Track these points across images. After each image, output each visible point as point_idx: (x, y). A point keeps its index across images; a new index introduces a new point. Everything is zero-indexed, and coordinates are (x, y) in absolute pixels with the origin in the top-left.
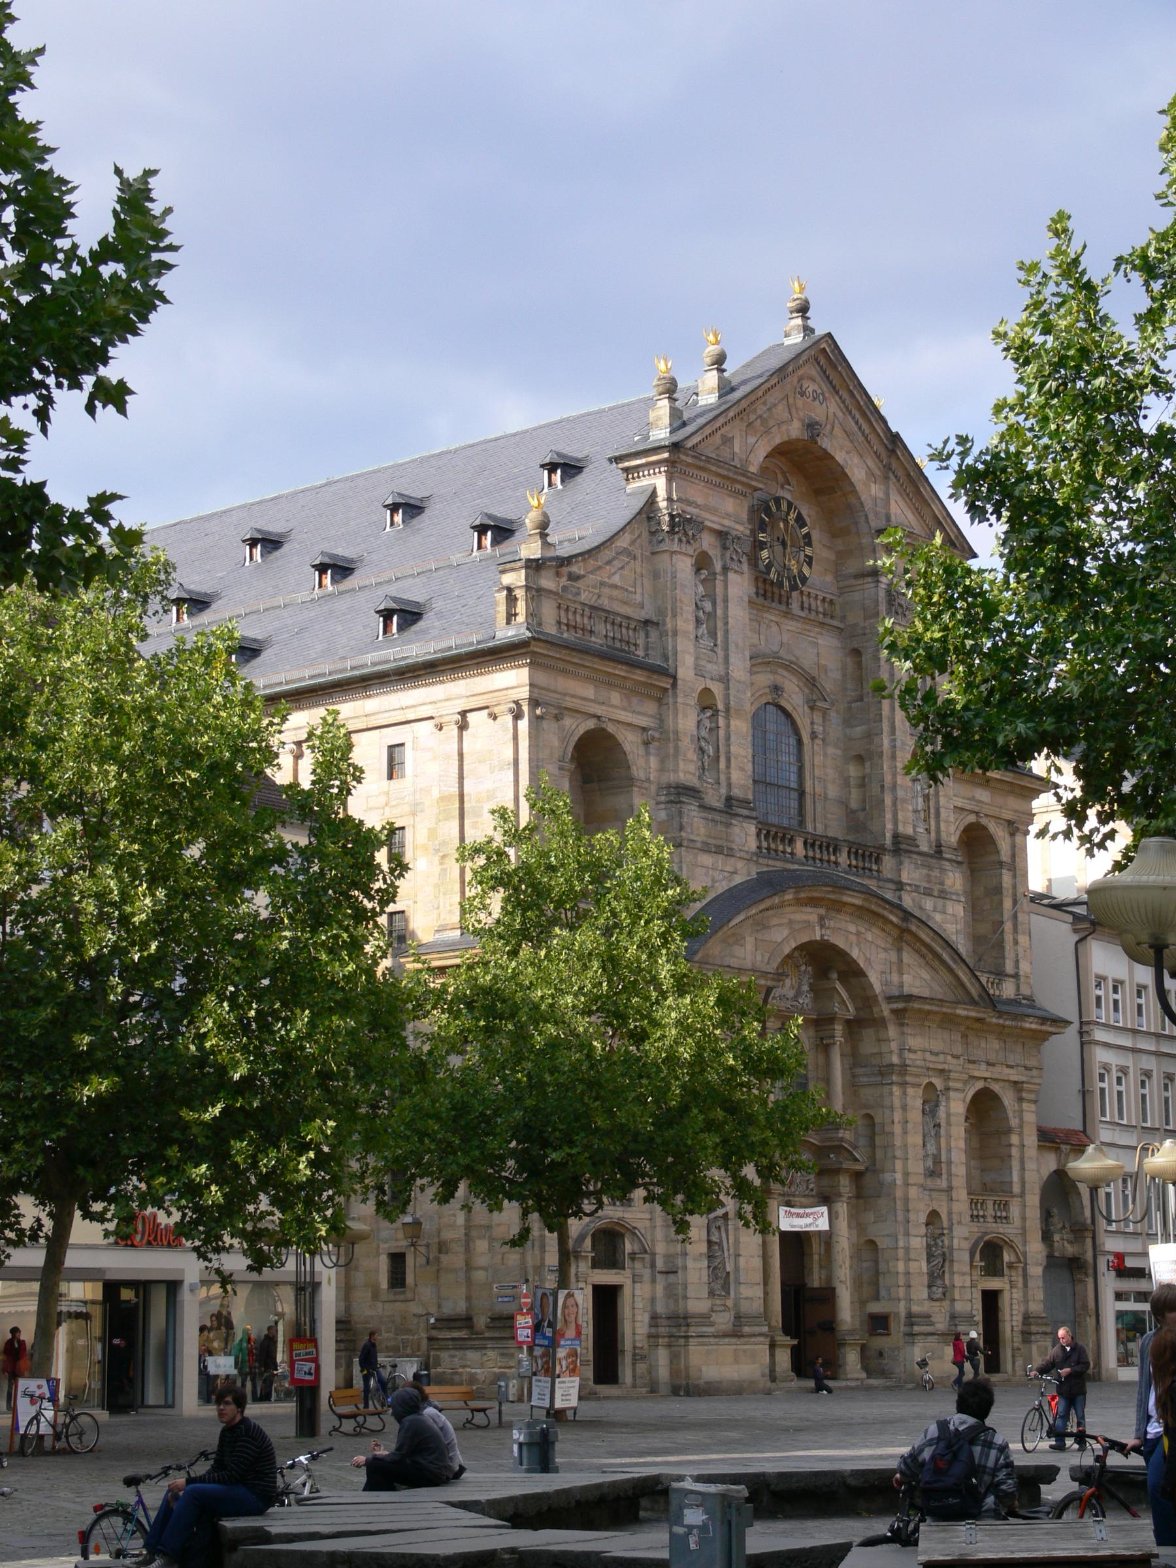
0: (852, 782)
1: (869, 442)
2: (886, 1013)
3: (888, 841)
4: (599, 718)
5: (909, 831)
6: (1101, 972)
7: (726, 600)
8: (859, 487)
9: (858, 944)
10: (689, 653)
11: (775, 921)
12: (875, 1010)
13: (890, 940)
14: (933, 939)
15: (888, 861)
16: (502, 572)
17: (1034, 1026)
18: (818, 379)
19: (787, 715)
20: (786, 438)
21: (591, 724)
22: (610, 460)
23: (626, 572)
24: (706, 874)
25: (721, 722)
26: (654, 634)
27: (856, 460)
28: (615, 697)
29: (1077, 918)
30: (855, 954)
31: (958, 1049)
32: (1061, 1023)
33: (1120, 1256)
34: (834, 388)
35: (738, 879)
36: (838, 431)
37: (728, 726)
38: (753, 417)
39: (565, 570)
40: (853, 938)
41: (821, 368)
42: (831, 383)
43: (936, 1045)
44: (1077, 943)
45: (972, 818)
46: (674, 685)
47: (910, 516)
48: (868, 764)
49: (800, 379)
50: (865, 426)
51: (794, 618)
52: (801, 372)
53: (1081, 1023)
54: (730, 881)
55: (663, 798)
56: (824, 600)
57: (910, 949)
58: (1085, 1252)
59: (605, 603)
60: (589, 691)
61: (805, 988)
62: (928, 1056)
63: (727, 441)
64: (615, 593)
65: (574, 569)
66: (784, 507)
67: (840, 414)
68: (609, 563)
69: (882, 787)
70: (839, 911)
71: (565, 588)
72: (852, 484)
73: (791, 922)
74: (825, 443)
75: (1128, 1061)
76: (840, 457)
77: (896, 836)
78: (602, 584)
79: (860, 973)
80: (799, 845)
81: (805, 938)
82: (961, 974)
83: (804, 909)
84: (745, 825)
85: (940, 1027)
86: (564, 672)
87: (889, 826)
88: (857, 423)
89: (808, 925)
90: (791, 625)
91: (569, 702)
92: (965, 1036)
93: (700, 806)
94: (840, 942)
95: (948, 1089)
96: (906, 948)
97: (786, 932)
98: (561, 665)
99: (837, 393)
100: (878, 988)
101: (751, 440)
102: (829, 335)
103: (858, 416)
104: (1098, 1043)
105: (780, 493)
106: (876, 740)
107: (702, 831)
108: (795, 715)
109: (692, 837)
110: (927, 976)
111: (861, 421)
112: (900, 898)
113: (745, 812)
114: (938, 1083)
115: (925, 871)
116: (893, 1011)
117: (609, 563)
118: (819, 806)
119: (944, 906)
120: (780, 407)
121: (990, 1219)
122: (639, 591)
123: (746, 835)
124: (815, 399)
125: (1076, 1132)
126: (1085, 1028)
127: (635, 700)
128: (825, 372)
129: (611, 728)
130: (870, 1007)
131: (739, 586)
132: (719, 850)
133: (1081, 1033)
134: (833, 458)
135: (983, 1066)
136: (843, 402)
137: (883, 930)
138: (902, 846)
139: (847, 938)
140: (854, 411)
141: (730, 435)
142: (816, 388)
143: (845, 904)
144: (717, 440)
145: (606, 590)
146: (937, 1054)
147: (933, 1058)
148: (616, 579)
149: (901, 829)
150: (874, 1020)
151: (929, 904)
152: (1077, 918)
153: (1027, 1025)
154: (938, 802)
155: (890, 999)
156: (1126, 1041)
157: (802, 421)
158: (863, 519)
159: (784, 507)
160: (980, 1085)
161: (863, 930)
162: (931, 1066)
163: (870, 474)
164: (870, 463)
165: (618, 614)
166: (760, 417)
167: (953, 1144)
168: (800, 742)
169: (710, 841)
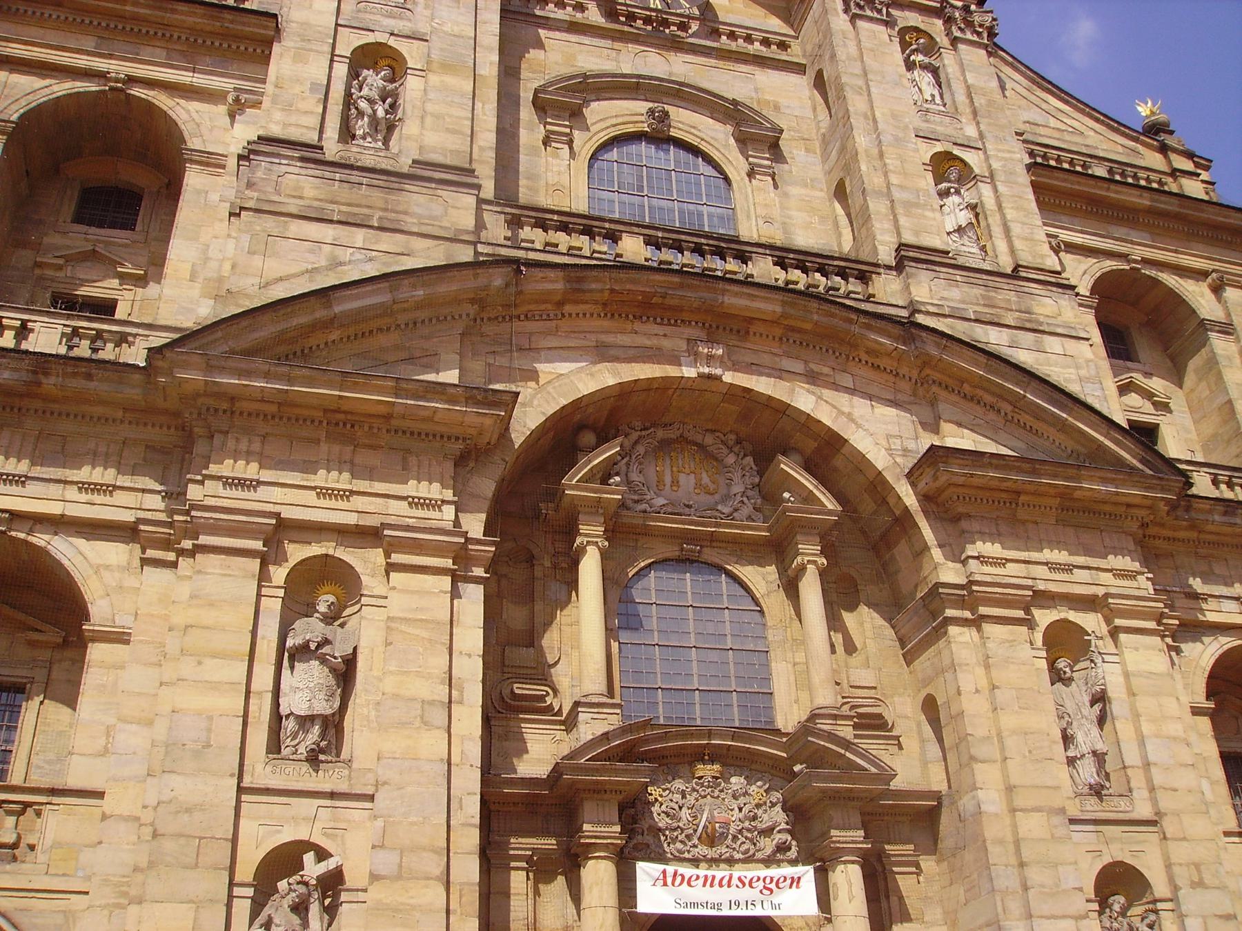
12: (891, 501)
13: (905, 386)
14: (988, 369)
24: (311, 251)
57: (954, 398)
69: (864, 191)
79: (833, 442)
83: (638, 326)
84: (439, 192)
93: (302, 159)
95: (1114, 633)
96: (943, 394)
100: (879, 459)
108: (704, 147)
109: (276, 198)
114: (1091, 622)
115: (977, 291)
130: (884, 502)
149: (909, 238)
154: (1003, 216)
161: (826, 370)
167: (1146, 728)
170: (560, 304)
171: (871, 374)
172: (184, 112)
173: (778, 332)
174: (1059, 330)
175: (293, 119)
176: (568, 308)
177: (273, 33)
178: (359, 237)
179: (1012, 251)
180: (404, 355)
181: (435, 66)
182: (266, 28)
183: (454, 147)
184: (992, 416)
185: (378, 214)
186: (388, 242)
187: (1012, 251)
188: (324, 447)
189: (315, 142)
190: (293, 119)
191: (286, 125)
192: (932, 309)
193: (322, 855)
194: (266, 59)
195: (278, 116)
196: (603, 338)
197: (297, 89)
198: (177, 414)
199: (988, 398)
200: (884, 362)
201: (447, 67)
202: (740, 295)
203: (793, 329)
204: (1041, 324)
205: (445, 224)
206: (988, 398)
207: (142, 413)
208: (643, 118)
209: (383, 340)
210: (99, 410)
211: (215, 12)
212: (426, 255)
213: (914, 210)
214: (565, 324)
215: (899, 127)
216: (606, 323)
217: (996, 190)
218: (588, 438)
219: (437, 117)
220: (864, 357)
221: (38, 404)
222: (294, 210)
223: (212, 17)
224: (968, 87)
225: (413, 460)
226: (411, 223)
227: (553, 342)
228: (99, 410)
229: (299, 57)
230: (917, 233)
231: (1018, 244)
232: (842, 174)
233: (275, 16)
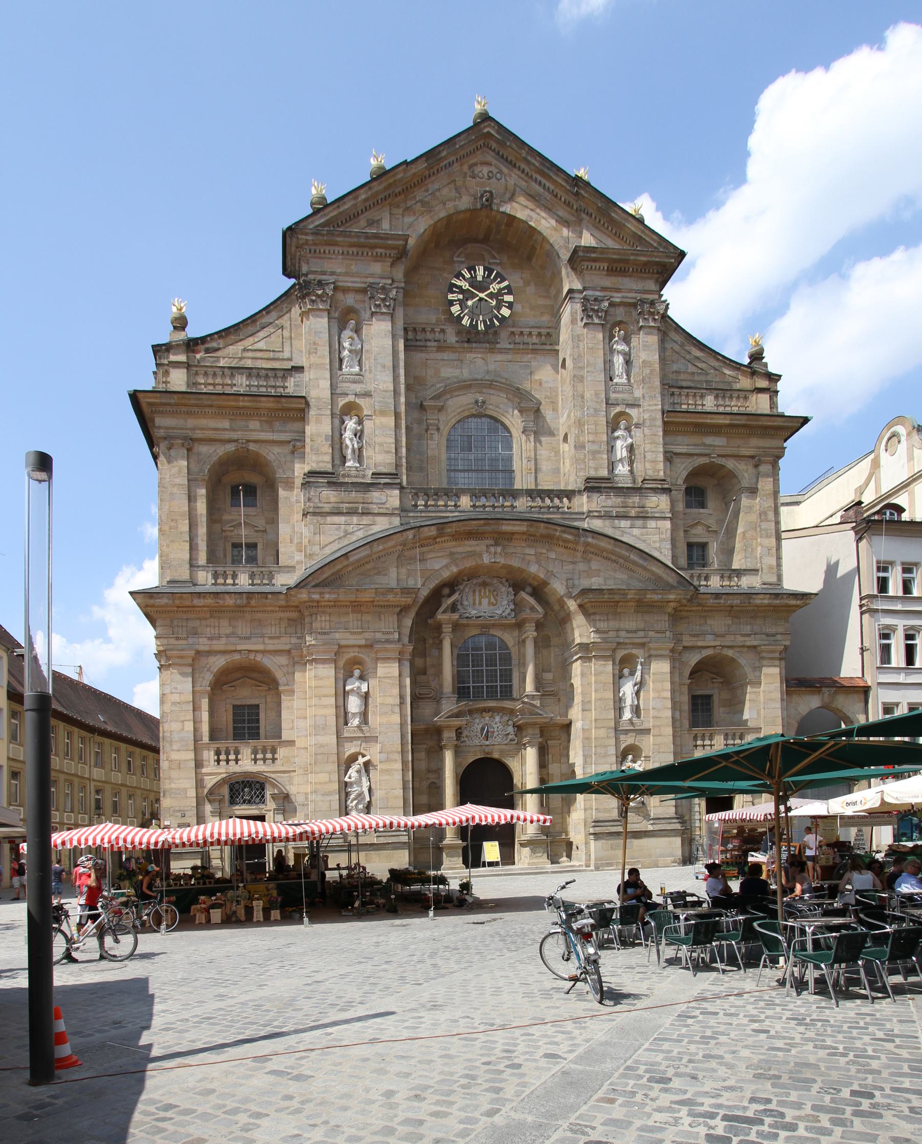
1: (556, 196)
4: (236, 441)
9: (538, 562)
10: (325, 379)
28: (254, 424)
34: (511, 163)
35: (376, 529)
38: (409, 203)
40: (533, 558)
41: (494, 151)
42: (506, 160)
43: (632, 625)
49: (471, 166)
50: (548, 184)
51: (501, 351)
54: (367, 531)
56: (540, 334)
59: (249, 363)
60: (226, 424)
62: (622, 634)
64: (259, 355)
65: (214, 345)
73: (452, 554)
76: (521, 214)
81: (469, 564)
83: (467, 542)
85: (636, 612)
88: (540, 184)
89: (472, 554)
90: (499, 357)
91: (199, 434)
94: (515, 563)
96: (594, 557)
97: (445, 561)
99: (515, 166)
101: (408, 220)
103: (539, 178)
110: (625, 577)
111: (544, 181)
120: (445, 191)
123: (393, 498)
124: (489, 178)
127: (277, 425)
128: (498, 153)
132: (351, 512)
134: (515, 217)
136: (523, 172)
137: (566, 548)
139: (524, 559)
140: (534, 175)
141: (376, 218)
142: (492, 168)
146: (635, 632)
147: (630, 635)
148: (261, 345)
151: (624, 523)
161: (544, 551)
166: (420, 201)
170: (435, 538)
171: (564, 550)
173: (525, 537)
174: (657, 515)
175: (320, 458)
176: (438, 540)
177: (303, 406)
178: (355, 519)
180: (376, 571)
181: (377, 413)
182: (301, 403)
183: (389, 461)
184: (615, 565)
185: (361, 506)
186: (366, 520)
188: (351, 616)
189: (330, 470)
190: (320, 458)
191: (318, 462)
192: (596, 514)
195: (314, 458)
196: (453, 550)
197: (320, 440)
198: (297, 607)
199: (614, 557)
200: (570, 545)
201: (383, 413)
202: (508, 525)
203: (530, 535)
204: (647, 513)
205: (388, 506)
206: (614, 557)
207: (284, 608)
209: (368, 566)
210: (270, 609)
211: (278, 399)
212: (381, 525)
213: (597, 456)
214: (437, 546)
215: (597, 402)
216: (454, 543)
218: (446, 591)
219: (381, 445)
220: (561, 543)
221: (249, 609)
223: (278, 402)
225: (382, 617)
226: (375, 509)
227: (432, 555)
228: (270, 609)
229: (318, 422)
230: (596, 469)
232: (567, 430)
233: (304, 397)
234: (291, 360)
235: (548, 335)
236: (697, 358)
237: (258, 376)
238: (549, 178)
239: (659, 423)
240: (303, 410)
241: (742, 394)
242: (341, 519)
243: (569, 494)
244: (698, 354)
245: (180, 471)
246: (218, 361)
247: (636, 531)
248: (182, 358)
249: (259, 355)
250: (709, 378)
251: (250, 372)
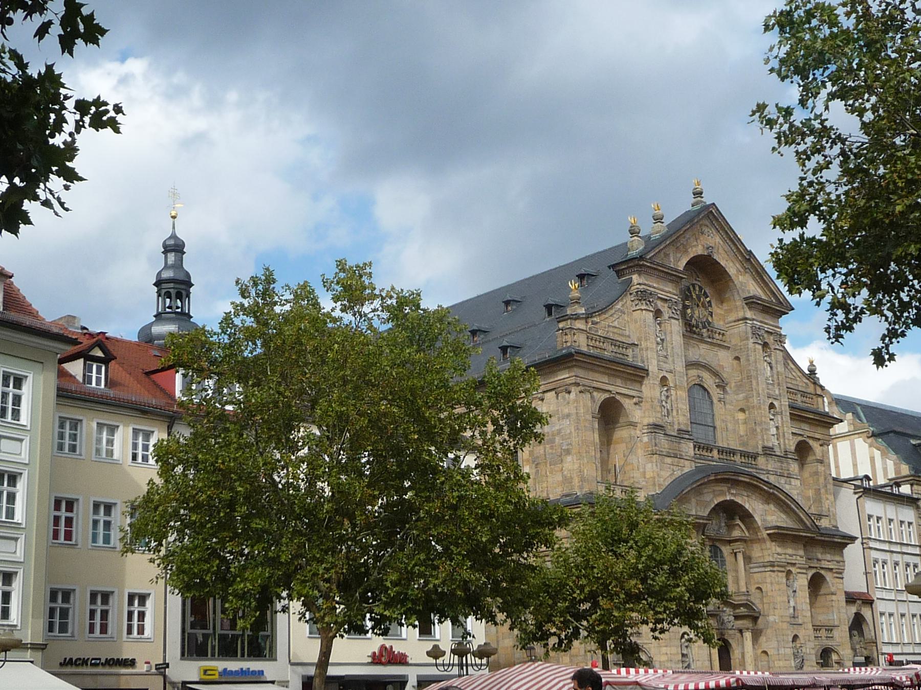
0: (740, 422)
2: (765, 536)
3: (760, 451)
5: (770, 445)
6: (871, 513)
7: (671, 333)
8: (733, 277)
11: (706, 491)
15: (761, 461)
16: (559, 322)
17: (839, 540)
18: (709, 224)
19: (705, 389)
20: (695, 254)
21: (607, 395)
22: (609, 267)
23: (620, 320)
25: (673, 392)
26: (637, 350)
27: (731, 264)
28: (619, 382)
29: (856, 487)
30: (747, 506)
31: (801, 552)
32: (853, 539)
33: (891, 655)
35: (686, 470)
36: (721, 250)
37: (676, 394)
39: (590, 320)
44: (858, 498)
45: (800, 438)
46: (648, 374)
47: (759, 291)
48: (747, 412)
49: (701, 226)
52: (701, 223)
53: (862, 538)
54: (682, 471)
55: (645, 431)
58: (873, 654)
59: (611, 335)
60: (605, 379)
61: (723, 524)
62: (788, 557)
63: (667, 255)
64: (615, 330)
66: (697, 288)
67: (721, 243)
68: (611, 316)
70: (738, 485)
71: (590, 328)
72: (730, 276)
73: (714, 491)
74: (715, 257)
75: (887, 556)
77: (764, 447)
78: (609, 326)
79: (750, 516)
80: (715, 452)
82: (801, 515)
86: (592, 370)
87: (760, 442)
92: (805, 546)
98: (589, 366)
101: (679, 255)
102: (714, 204)
104: (871, 548)
105: (695, 282)
106: (751, 400)
107: (666, 446)
108: (709, 390)
111: (732, 246)
112: (768, 478)
113: (687, 437)
116: (768, 534)
117: (611, 316)
118: (724, 433)
119: (790, 481)
121: (823, 638)
122: (627, 329)
123: (688, 448)
125: (864, 593)
126: (864, 541)
129: (618, 397)
131: (675, 328)
133: (862, 544)
135: (815, 561)
138: (768, 452)
143: (741, 481)
144: (662, 254)
145: (611, 329)
148: (616, 324)
149: (766, 444)
150: (759, 539)
151: (783, 480)
152: (856, 487)
153: (836, 540)
155: (767, 529)
156: (886, 547)
157: (703, 246)
158: (736, 293)
159: (697, 288)
160: (814, 571)
162: (789, 561)
163: (738, 271)
164: (738, 265)
165: (618, 341)
168: (712, 402)
169: (670, 451)
172: (627, 403)
179: (785, 444)
187: (785, 444)
193: (688, 635)
194: (641, 383)
208: (694, 378)
217: (782, 419)
222: (664, 453)
224: (778, 372)
231: (787, 441)
234: (629, 336)
235: (723, 335)
236: (792, 369)
237: (615, 346)
238: (735, 245)
239: (788, 414)
240: (643, 377)
241: (811, 396)
242: (669, 460)
243: (755, 456)
244: (793, 366)
245: (588, 410)
246: (597, 331)
247: (787, 487)
248: (583, 327)
249: (615, 330)
250: (798, 383)
251: (614, 342)
